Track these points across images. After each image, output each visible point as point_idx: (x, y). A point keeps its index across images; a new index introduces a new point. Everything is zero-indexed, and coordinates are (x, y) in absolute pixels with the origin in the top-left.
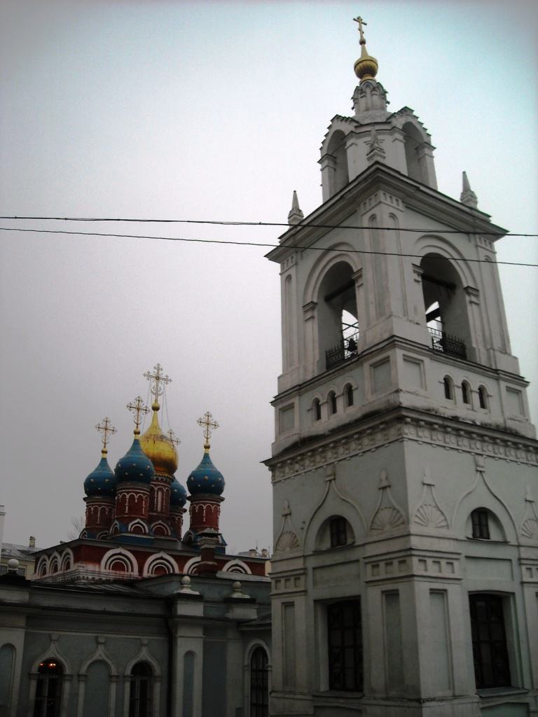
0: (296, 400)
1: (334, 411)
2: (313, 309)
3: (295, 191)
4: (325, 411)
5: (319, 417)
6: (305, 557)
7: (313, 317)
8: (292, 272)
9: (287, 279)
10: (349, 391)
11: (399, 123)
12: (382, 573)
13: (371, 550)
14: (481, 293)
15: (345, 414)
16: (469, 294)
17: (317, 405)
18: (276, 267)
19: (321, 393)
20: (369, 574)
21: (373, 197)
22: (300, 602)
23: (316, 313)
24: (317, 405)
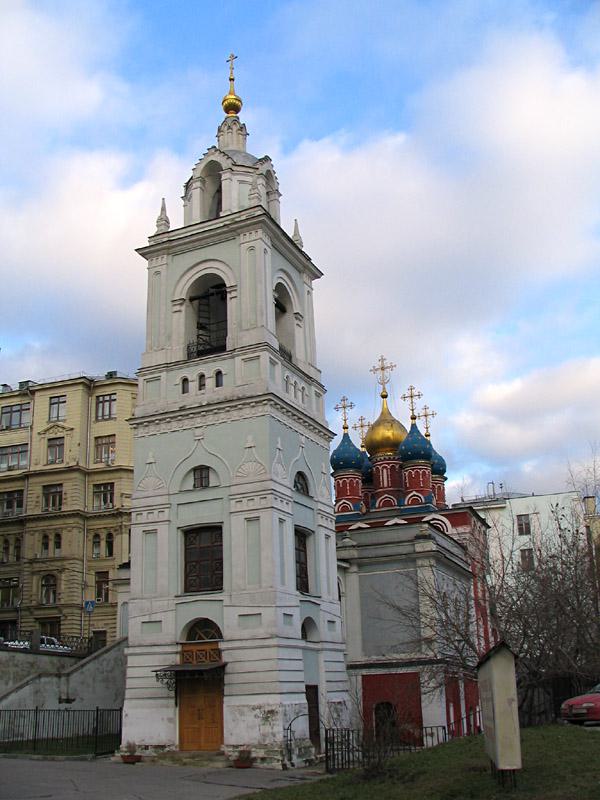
0: (163, 375)
1: (202, 386)
2: (181, 304)
4: (193, 386)
5: (185, 390)
6: (169, 495)
7: (180, 311)
8: (163, 269)
9: (154, 274)
10: (219, 374)
11: (263, 169)
12: (245, 505)
13: (234, 490)
14: (306, 317)
15: (211, 392)
16: (297, 318)
17: (185, 381)
18: (144, 263)
19: (192, 373)
20: (234, 506)
21: (253, 232)
22: (162, 529)
23: (183, 308)
24: (185, 381)
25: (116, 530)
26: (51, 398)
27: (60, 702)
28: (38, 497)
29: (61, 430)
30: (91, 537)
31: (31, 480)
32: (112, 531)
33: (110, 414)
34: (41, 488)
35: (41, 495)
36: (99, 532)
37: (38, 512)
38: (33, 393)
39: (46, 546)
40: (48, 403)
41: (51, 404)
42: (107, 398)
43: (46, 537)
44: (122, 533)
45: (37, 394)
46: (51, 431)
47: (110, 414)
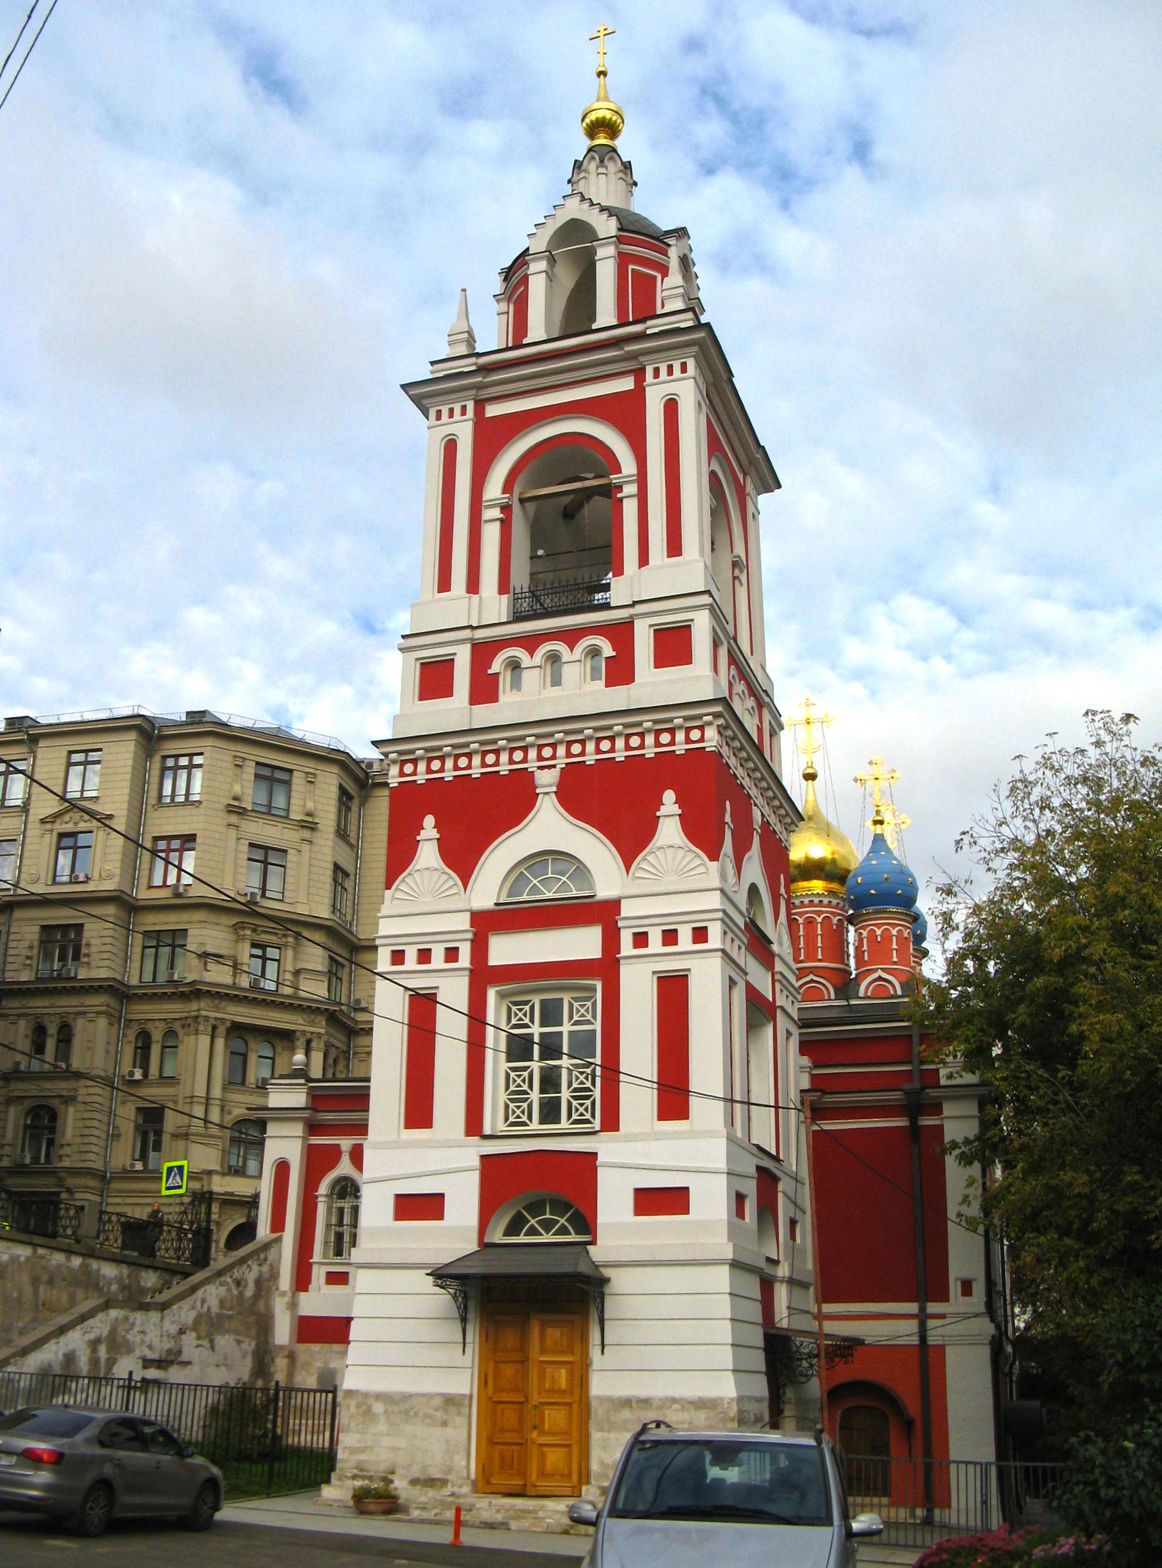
3: (464, 290)
25: (183, 1027)
26: (71, 753)
27: (145, 1367)
28: (31, 947)
29: (86, 817)
30: (131, 1035)
31: (18, 914)
32: (177, 1026)
33: (188, 794)
34: (37, 929)
35: (36, 944)
36: (150, 1027)
37: (25, 976)
38: (34, 740)
39: (39, 1048)
40: (64, 761)
41: (70, 764)
42: (184, 761)
43: (40, 1031)
44: (197, 1033)
45: (42, 743)
46: (67, 818)
47: (188, 794)
